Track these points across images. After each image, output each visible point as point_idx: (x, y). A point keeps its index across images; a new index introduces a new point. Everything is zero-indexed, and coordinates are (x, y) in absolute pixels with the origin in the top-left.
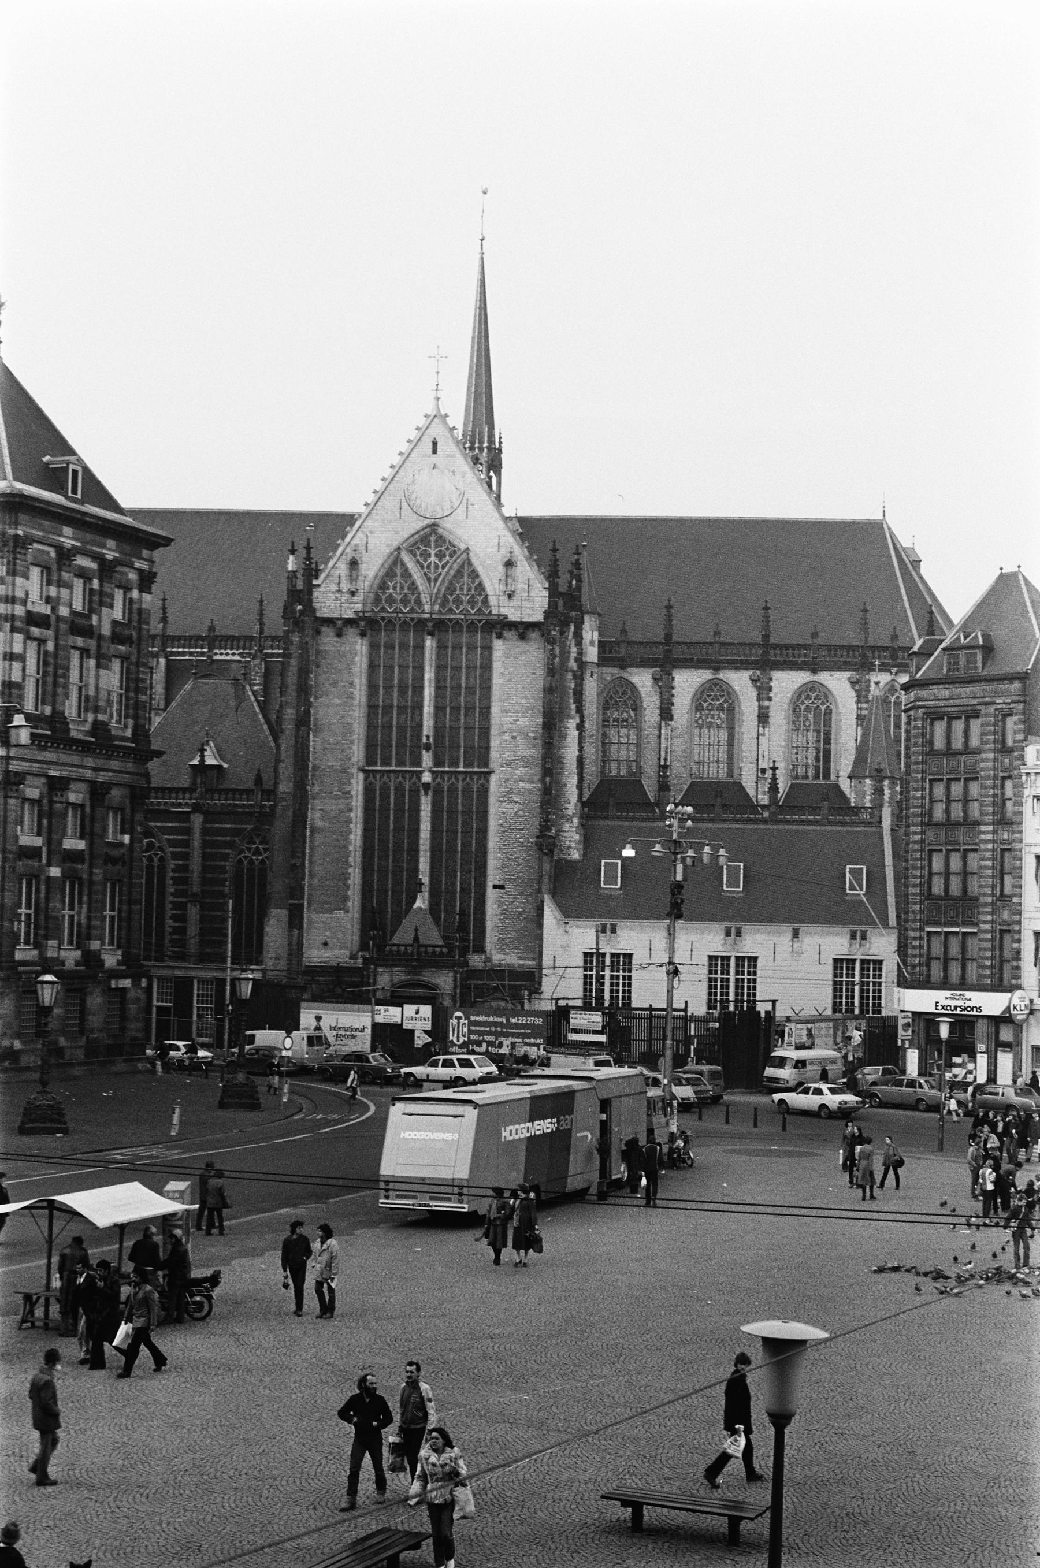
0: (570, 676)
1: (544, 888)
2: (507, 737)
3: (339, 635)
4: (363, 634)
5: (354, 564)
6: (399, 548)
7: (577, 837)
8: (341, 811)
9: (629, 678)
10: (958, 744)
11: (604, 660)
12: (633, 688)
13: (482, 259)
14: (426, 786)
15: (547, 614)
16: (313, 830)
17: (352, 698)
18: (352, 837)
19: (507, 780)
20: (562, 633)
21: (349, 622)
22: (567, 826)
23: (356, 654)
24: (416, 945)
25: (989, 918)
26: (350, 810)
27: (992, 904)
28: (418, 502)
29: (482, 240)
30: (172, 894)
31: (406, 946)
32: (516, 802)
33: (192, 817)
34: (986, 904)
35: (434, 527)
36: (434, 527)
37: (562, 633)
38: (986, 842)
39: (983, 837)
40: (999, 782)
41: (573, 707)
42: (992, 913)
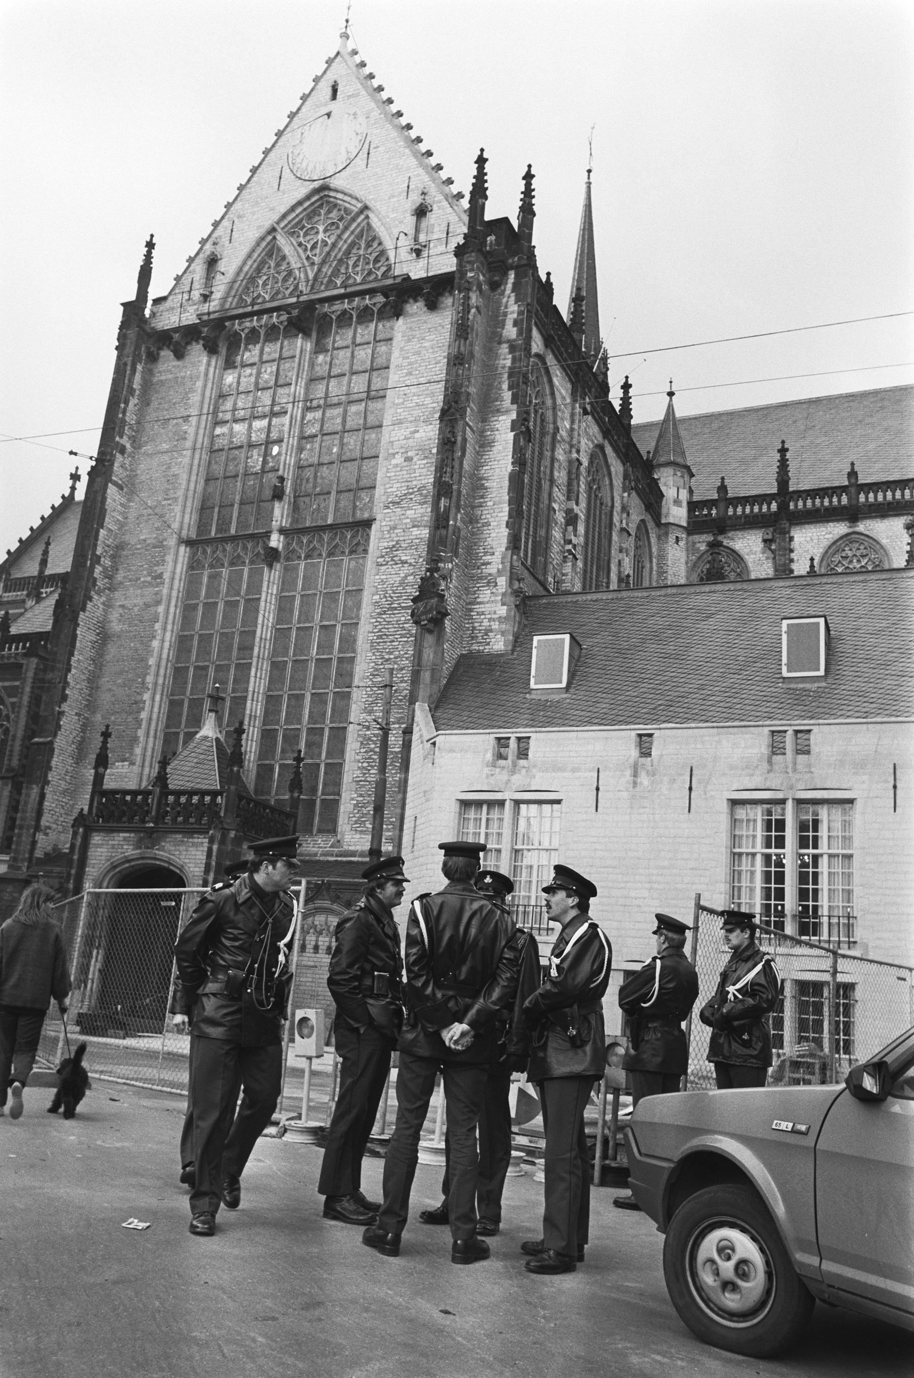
0: (504, 349)
1: (423, 693)
2: (399, 460)
4: (212, 349)
5: (212, 262)
6: (273, 230)
7: (503, 611)
8: (147, 605)
9: (731, 544)
11: (695, 526)
12: (737, 557)
13: (589, 188)
14: (272, 556)
16: (104, 637)
17: (185, 439)
18: (155, 644)
19: (394, 528)
21: (190, 333)
22: (485, 594)
23: (198, 377)
26: (158, 603)
29: (589, 171)
32: (404, 562)
35: (323, 189)
36: (323, 189)
37: (495, 286)
41: (507, 395)
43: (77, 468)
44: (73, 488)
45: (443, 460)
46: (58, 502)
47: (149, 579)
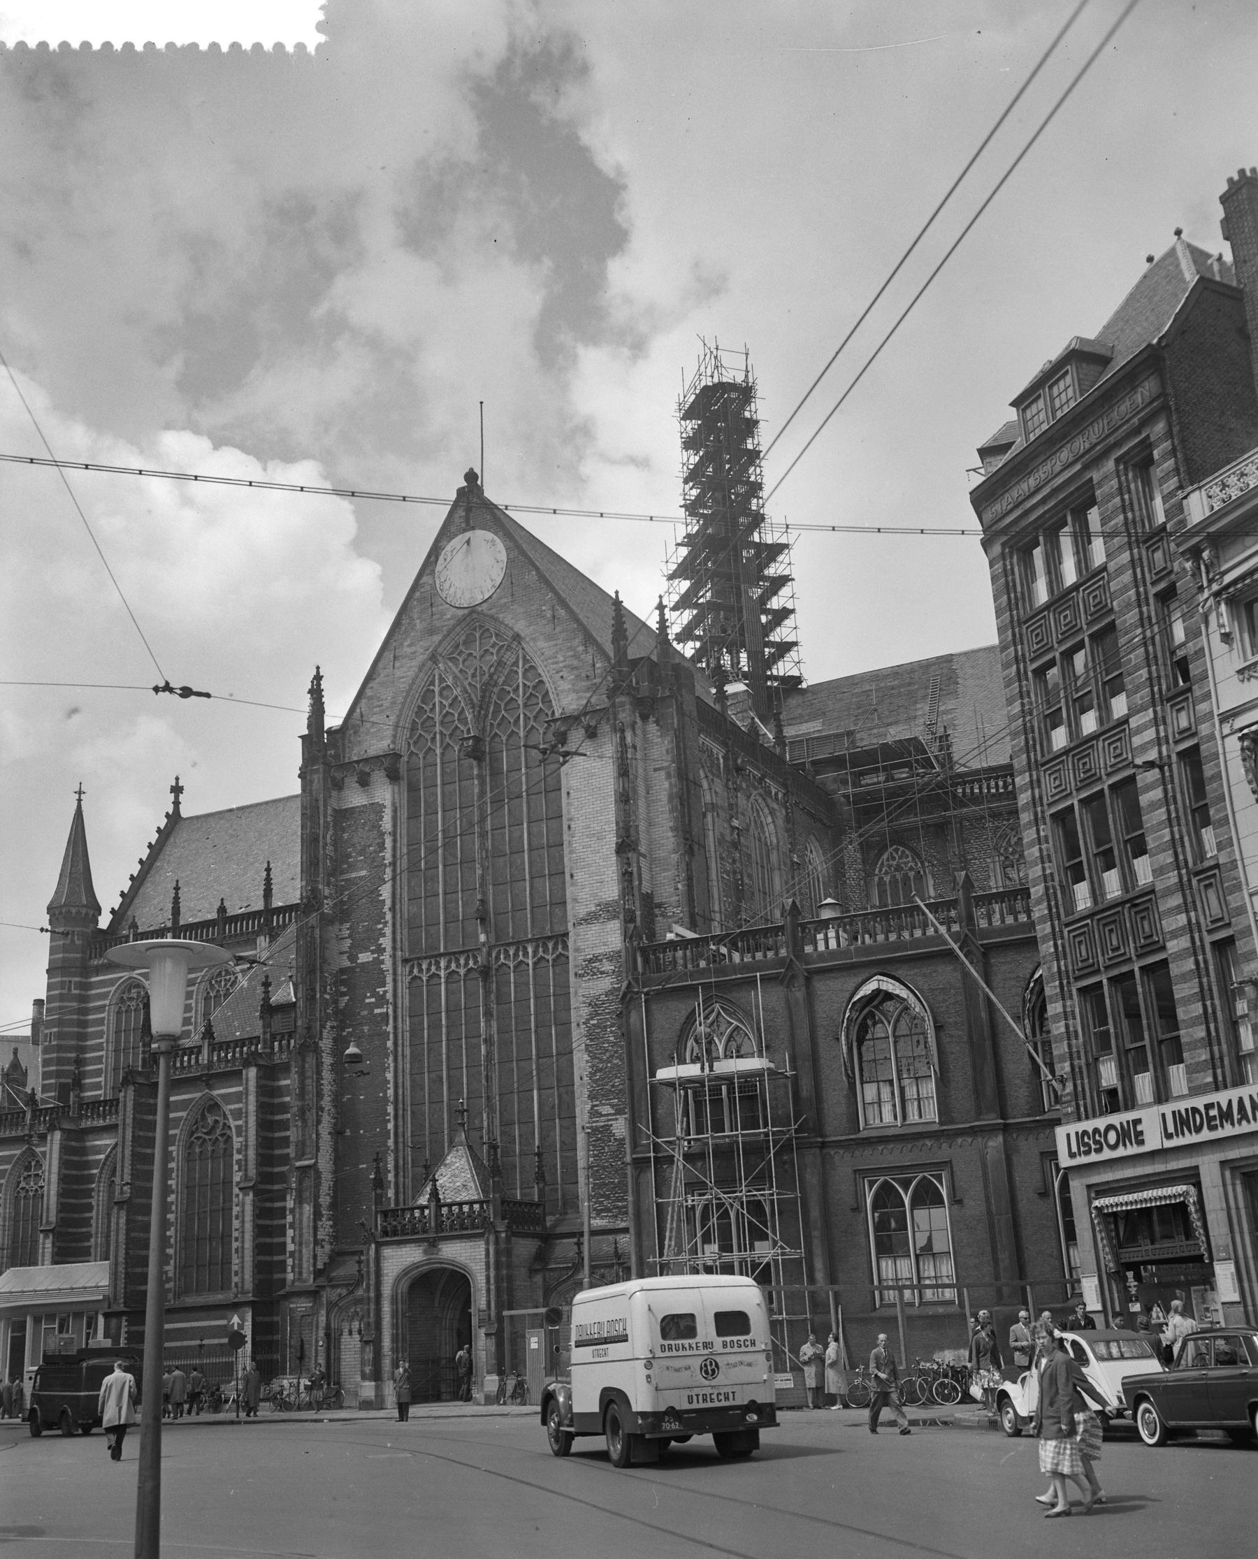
3: (364, 782)
10: (1070, 575)
15: (612, 694)
20: (645, 718)
24: (433, 1204)
25: (1182, 919)
27: (1181, 886)
28: (452, 590)
30: (238, 1183)
31: (422, 1208)
33: (244, 1072)
34: (1168, 892)
38: (1144, 748)
39: (1137, 741)
40: (1152, 608)
42: (1185, 908)
43: (177, 779)
44: (177, 803)
45: (624, 889)
46: (162, 823)
47: (373, 1000)
